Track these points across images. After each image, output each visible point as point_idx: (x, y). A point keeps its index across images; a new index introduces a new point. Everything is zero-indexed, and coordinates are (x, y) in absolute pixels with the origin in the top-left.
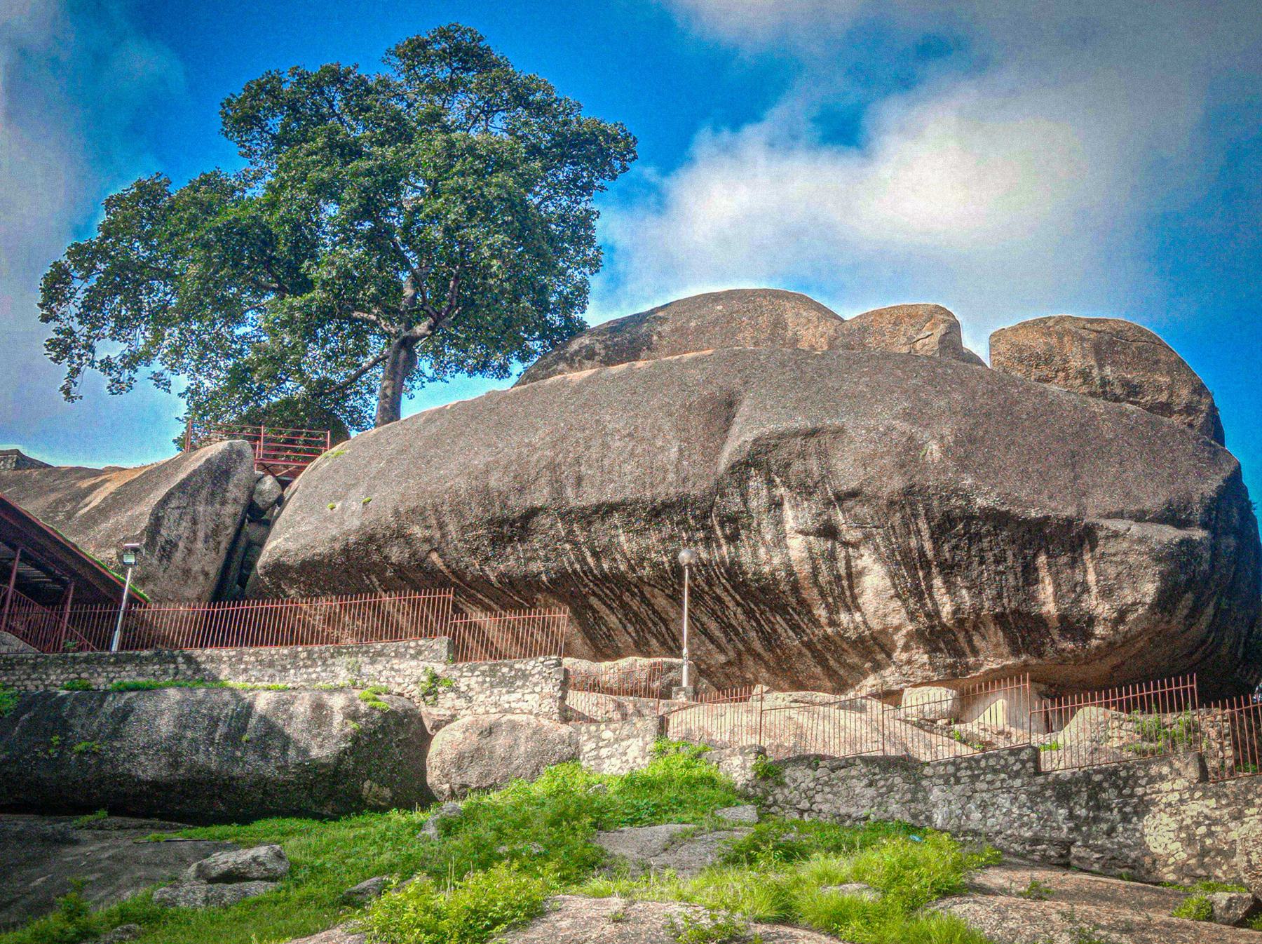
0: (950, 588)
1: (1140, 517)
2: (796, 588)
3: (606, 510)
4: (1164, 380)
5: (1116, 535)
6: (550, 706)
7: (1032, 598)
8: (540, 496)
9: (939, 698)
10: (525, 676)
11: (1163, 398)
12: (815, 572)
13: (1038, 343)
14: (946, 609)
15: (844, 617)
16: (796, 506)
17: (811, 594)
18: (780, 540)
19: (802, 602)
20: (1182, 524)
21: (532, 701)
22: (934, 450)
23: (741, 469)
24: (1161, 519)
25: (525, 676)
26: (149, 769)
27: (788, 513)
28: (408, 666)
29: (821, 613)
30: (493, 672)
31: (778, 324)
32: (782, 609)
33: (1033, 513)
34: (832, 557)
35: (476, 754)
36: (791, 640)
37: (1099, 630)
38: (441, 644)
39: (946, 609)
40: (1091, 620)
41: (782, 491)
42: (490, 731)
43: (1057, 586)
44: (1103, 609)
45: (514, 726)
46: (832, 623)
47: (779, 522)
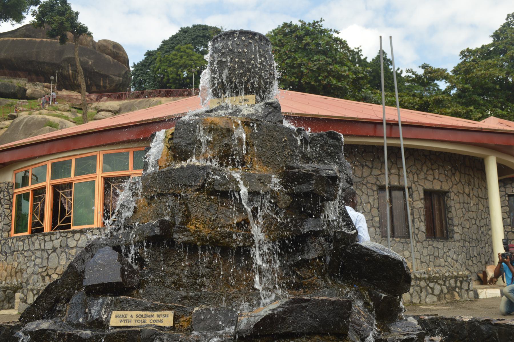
0: (90, 80)
1: (114, 75)
2: (69, 77)
4: (122, 53)
5: (111, 77)
6: (41, 89)
7: (100, 83)
10: (38, 85)
11: (121, 55)
12: (72, 76)
13: (105, 44)
14: (89, 83)
15: (75, 82)
16: (71, 67)
17: (71, 78)
18: (68, 71)
19: (70, 79)
20: (119, 77)
21: (39, 88)
22: (90, 63)
23: (64, 60)
24: (116, 76)
25: (38, 85)
27: (70, 69)
28: (21, 81)
29: (72, 81)
30: (34, 84)
33: (101, 73)
34: (75, 74)
35: (33, 93)
36: (67, 83)
38: (27, 80)
39: (89, 83)
40: (106, 86)
41: (70, 65)
42: (35, 91)
43: (103, 82)
44: (108, 86)
45: (37, 91)
46: (74, 82)
47: (69, 68)
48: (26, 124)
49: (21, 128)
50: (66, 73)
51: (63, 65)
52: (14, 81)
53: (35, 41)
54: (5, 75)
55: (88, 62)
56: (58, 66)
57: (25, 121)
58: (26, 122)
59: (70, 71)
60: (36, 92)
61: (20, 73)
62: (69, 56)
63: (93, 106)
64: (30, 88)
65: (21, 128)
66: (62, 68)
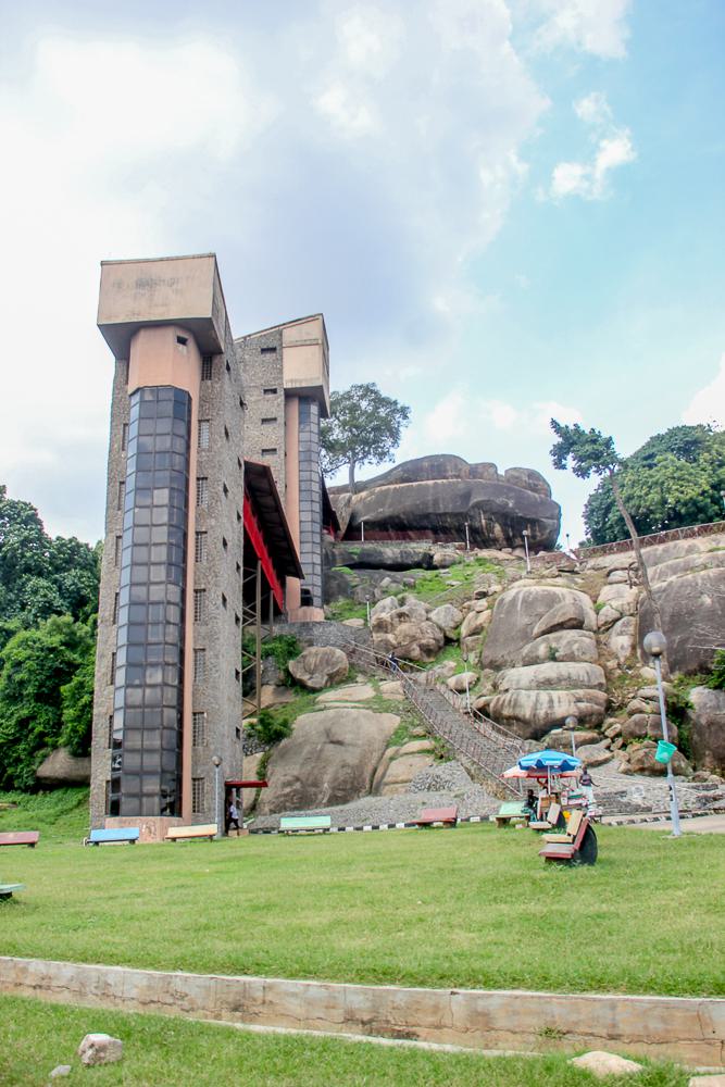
3: (445, 514)
8: (431, 510)
9: (510, 550)
13: (516, 474)
14: (511, 534)
17: (485, 531)
20: (552, 519)
22: (511, 505)
23: (473, 507)
26: (389, 562)
31: (456, 465)
32: (478, 533)
35: (445, 560)
37: (538, 538)
39: (511, 534)
44: (538, 534)
48: (524, 601)
49: (519, 608)
50: (477, 524)
51: (472, 513)
52: (414, 545)
53: (427, 486)
54: (391, 539)
55: (507, 504)
56: (465, 516)
57: (521, 596)
58: (524, 598)
59: (483, 521)
60: (447, 558)
61: (410, 533)
62: (480, 499)
63: (589, 566)
64: (439, 553)
65: (519, 608)
66: (472, 518)
